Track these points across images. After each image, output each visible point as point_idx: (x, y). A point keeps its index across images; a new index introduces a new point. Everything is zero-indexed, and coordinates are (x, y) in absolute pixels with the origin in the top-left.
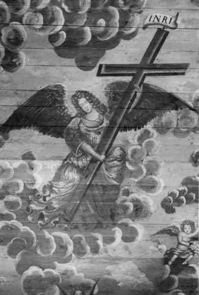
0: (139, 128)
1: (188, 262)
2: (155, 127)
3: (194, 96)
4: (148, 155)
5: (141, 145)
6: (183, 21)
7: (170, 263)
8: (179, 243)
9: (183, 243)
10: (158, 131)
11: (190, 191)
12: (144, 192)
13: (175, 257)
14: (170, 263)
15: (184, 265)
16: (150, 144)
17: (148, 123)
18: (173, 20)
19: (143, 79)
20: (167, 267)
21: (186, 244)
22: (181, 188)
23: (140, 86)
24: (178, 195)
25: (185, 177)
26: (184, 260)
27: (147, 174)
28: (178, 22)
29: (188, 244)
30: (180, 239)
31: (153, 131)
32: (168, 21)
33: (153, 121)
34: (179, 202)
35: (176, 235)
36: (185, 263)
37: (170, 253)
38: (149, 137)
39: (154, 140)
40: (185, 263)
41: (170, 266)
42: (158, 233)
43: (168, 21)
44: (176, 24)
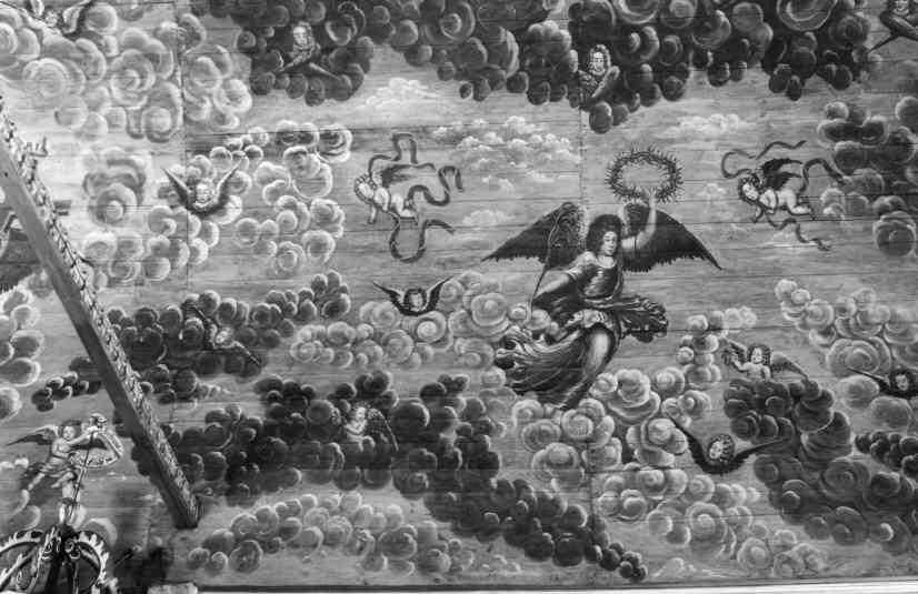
0: (6, 290)
1: (61, 484)
2: (30, 287)
3: (84, 242)
4: (19, 328)
5: (8, 314)
6: (54, 147)
7: (31, 486)
8: (52, 455)
9: (58, 454)
10: (35, 293)
11: (81, 378)
12: (8, 382)
13: (41, 475)
14: (31, 486)
15: (56, 488)
16: (23, 314)
17: (20, 282)
18: (40, 147)
19: (10, 221)
20: (25, 493)
21: (63, 455)
22: (70, 374)
23: (5, 231)
24: (62, 385)
25: (75, 356)
26: (56, 479)
27: (16, 356)
28: (48, 147)
29: (66, 456)
30: (54, 448)
31: (28, 294)
32: (34, 147)
33: (27, 279)
34: (60, 393)
35: (49, 443)
36: (57, 485)
37: (33, 471)
38: (21, 302)
39: (30, 308)
40: (57, 485)
41: (30, 492)
42: (18, 441)
43: (34, 147)
44: (44, 150)
